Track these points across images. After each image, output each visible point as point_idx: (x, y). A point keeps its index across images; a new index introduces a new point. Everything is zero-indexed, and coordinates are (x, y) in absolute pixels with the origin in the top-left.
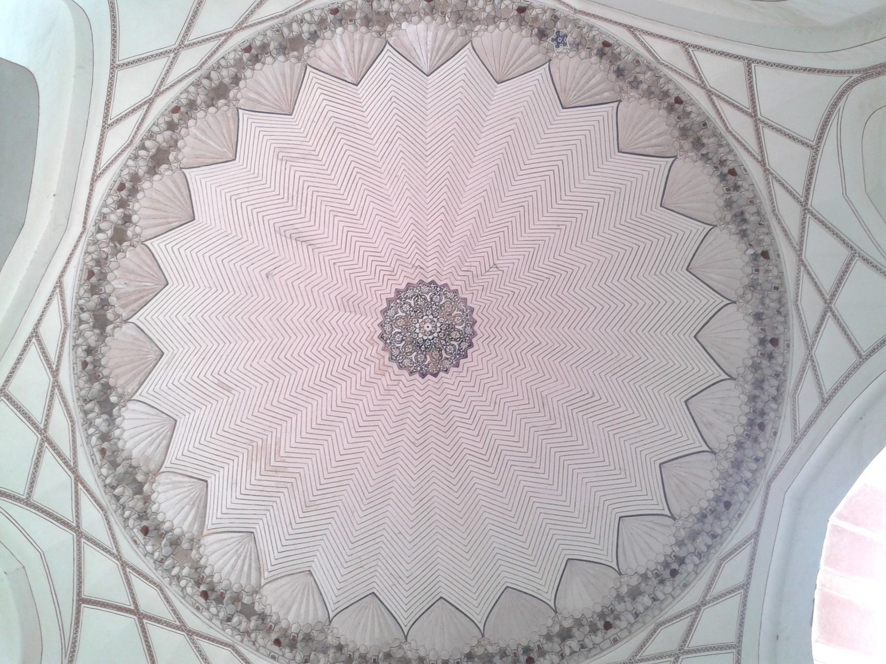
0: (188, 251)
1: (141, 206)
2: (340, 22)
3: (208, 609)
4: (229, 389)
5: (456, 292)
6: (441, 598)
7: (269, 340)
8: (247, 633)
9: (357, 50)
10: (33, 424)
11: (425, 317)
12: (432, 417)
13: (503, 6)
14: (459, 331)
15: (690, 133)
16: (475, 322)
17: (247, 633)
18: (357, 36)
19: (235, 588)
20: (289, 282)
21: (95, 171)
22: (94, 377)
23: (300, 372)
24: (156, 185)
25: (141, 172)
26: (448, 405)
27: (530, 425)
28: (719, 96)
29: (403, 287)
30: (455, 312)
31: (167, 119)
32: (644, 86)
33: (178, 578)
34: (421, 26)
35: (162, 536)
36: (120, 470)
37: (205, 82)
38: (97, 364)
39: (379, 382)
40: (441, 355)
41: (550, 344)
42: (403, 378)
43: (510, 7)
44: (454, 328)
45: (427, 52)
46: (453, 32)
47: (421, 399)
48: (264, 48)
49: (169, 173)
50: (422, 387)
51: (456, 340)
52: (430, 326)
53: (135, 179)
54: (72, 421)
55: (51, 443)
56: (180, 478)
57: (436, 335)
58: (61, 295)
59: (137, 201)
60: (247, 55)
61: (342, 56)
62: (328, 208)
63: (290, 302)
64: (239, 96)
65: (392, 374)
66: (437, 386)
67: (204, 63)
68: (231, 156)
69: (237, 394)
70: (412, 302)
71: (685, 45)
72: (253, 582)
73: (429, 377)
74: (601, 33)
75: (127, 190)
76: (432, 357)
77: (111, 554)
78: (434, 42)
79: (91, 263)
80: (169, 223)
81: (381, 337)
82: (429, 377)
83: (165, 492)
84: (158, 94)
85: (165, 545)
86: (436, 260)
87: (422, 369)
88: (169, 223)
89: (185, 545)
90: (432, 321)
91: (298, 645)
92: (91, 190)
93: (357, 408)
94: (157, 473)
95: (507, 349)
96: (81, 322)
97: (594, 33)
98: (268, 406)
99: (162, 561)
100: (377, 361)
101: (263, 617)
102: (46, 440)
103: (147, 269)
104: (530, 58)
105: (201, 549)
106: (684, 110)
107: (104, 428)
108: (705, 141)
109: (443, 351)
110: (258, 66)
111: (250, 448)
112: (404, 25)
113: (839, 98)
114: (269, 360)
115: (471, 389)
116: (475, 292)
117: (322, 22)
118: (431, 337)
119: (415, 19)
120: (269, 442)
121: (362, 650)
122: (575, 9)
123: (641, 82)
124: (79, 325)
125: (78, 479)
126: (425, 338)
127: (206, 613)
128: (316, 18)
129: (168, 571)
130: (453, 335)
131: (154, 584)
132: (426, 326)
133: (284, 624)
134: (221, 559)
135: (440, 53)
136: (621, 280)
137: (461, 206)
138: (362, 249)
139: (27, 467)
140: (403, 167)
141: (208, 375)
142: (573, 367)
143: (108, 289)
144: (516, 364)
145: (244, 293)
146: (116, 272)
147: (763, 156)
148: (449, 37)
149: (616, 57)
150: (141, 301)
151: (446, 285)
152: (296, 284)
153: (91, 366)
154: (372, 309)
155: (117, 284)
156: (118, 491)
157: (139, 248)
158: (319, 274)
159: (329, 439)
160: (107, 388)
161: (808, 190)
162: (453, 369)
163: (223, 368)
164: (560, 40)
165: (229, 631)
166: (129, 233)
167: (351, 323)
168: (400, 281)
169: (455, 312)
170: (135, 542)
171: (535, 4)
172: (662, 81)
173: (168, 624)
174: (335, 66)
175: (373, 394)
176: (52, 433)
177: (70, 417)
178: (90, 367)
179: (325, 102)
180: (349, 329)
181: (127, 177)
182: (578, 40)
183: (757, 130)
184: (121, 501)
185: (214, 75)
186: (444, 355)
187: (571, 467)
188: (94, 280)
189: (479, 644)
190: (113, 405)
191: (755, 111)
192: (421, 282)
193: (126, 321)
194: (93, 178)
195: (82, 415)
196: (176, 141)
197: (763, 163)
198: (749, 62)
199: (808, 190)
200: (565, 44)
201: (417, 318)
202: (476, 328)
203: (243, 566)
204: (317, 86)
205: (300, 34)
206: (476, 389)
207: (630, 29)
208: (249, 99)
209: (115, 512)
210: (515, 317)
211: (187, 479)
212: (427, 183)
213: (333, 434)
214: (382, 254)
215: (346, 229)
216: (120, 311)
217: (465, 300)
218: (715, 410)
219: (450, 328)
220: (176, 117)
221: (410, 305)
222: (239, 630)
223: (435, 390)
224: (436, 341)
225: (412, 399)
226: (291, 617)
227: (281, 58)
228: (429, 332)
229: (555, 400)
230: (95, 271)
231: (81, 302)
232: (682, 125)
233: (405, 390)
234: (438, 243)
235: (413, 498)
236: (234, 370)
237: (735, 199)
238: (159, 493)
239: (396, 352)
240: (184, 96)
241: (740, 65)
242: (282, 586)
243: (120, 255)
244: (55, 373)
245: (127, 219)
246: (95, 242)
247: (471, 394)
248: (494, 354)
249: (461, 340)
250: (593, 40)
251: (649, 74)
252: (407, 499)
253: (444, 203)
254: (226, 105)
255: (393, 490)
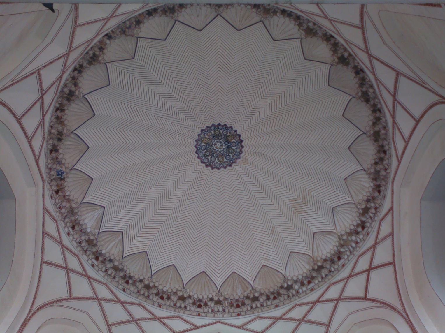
0: (219, 265)
1: (205, 295)
2: (101, 254)
3: (368, 227)
4: (273, 229)
5: (197, 141)
6: (343, 115)
7: (247, 217)
8: (376, 208)
9: (109, 239)
10: (297, 327)
11: (214, 148)
12: (260, 132)
13: (60, 201)
14: (214, 132)
15: (68, 97)
16: (207, 127)
17: (376, 208)
18: (103, 243)
19: (358, 215)
20: (219, 216)
21: (193, 329)
22: (279, 294)
23: (257, 199)
24: (195, 292)
25: (191, 301)
26: (251, 126)
27: (246, 88)
28: (43, 112)
29: (204, 165)
30: (207, 136)
31: (166, 301)
32: (60, 127)
33: (356, 243)
34: (86, 222)
35: (340, 252)
36: (314, 274)
37: (146, 294)
38: (273, 293)
39: (251, 161)
40: (229, 136)
41: (203, 92)
42: (246, 150)
43: (58, 198)
44: (214, 134)
45: (95, 213)
46: (82, 209)
47: (253, 139)
48: (124, 278)
49: (188, 290)
50: (247, 140)
51: (220, 132)
52: (218, 144)
53: (194, 303)
54: (296, 306)
55: (304, 317)
56: (315, 246)
57: (221, 140)
58: (246, 324)
59: (203, 298)
60: (130, 281)
61: (113, 243)
62: (181, 212)
63: (228, 213)
64: (146, 277)
65: (246, 156)
66: (244, 133)
67: (137, 304)
68: (173, 267)
69: (275, 224)
70: (209, 158)
71: (29, 142)
72: (354, 206)
73: (241, 138)
74: (47, 159)
75: (200, 304)
76: (232, 139)
77: (347, 282)
78: (89, 212)
79: (233, 308)
80: (209, 281)
81: (231, 166)
82: (241, 138)
83: (322, 251)
84: (156, 318)
85: (344, 249)
86: (186, 156)
87: (239, 143)
88: (209, 281)
89: (342, 242)
90: (215, 144)
91: (378, 183)
92: (201, 327)
93: (266, 168)
94: (313, 258)
95: (214, 109)
96: (257, 307)
97: (49, 161)
98: (277, 208)
99: (350, 251)
100: (242, 164)
101: (368, 201)
102: (303, 320)
103: (230, 283)
104: (76, 174)
105: (343, 233)
106: (60, 106)
107: (299, 284)
108: (68, 92)
109: (227, 135)
110: (132, 275)
111: (297, 213)
112: (89, 230)
113: (7, 87)
114: (256, 214)
115: (240, 118)
116: (193, 133)
117: (103, 262)
118: (223, 142)
119: (84, 227)
120: (292, 205)
121: (376, 151)
122: (43, 183)
123: (58, 131)
124: (258, 307)
125: (318, 301)
126: (224, 145)
127: (370, 230)
128: (103, 265)
129: (353, 248)
130: (217, 133)
131: (358, 259)
132: (218, 146)
133: (371, 189)
134: (347, 220)
135: (92, 208)
136: (156, 77)
137: (155, 158)
138: (193, 190)
139: (314, 327)
140: (150, 190)
141: (269, 239)
142: (209, 78)
143: (242, 297)
144: (219, 102)
145: (230, 234)
146: (235, 295)
147: (58, 80)
148: (84, 209)
149: (54, 146)
150: (244, 281)
151: (195, 147)
152: (219, 213)
153: (275, 295)
154: (219, 174)
155: (239, 294)
156: (324, 276)
157: (221, 291)
158: (211, 205)
159: (284, 177)
160: (282, 287)
161: (59, 58)
162: (234, 129)
163: (265, 233)
164: (60, 173)
165: (376, 218)
166: (216, 299)
167: (228, 182)
168: (202, 167)
169: (207, 136)
170: (344, 265)
171: (51, 192)
172: (52, 124)
173: (373, 254)
174: (119, 245)
175: (258, 162)
176: (300, 317)
177: (294, 307)
178: (276, 295)
179: (136, 238)
180: (231, 182)
181: (195, 306)
182: (56, 163)
183: (47, 91)
184: (327, 273)
185: (142, 292)
186: (229, 134)
187: (260, 64)
188: (240, 304)
189: (360, 98)
190: (288, 285)
191: (39, 99)
192: (198, 158)
193: (253, 288)
194: (197, 329)
195: (294, 298)
196: (174, 293)
197: (61, 77)
198: (19, 120)
199: (59, 58)
200: (61, 170)
201: (216, 152)
202: (210, 125)
203: (348, 210)
204: (130, 246)
205: (112, 268)
206: (239, 116)
207: (37, 162)
208: (147, 271)
209: (332, 277)
210: (197, 111)
211: (315, 242)
212: (152, 177)
213: (281, 176)
214: (192, 181)
215: (187, 201)
216: (249, 290)
217: (199, 135)
218: (198, 16)
219: (215, 136)
220: (165, 297)
221: (211, 158)
222: (375, 214)
223: (247, 134)
224: (223, 140)
225: (254, 143)
226: (367, 185)
227: (125, 268)
228: (220, 145)
229: (229, 81)
230: (236, 304)
231: (249, 308)
232: (67, 102)
233: (251, 148)
234: (177, 159)
235: (301, 132)
236: (265, 228)
237: (87, 62)
238: (323, 254)
239: (235, 157)
240: (155, 299)
241: (23, 121)
242: (354, 192)
243: (227, 297)
244: (277, 319)
245: (211, 299)
246: (224, 311)
247: (242, 118)
248: (219, 114)
249: (218, 129)
250: (53, 159)
251: (53, 131)
252: (302, 135)
253: (158, 165)
254: (152, 282)
255: (300, 143)
